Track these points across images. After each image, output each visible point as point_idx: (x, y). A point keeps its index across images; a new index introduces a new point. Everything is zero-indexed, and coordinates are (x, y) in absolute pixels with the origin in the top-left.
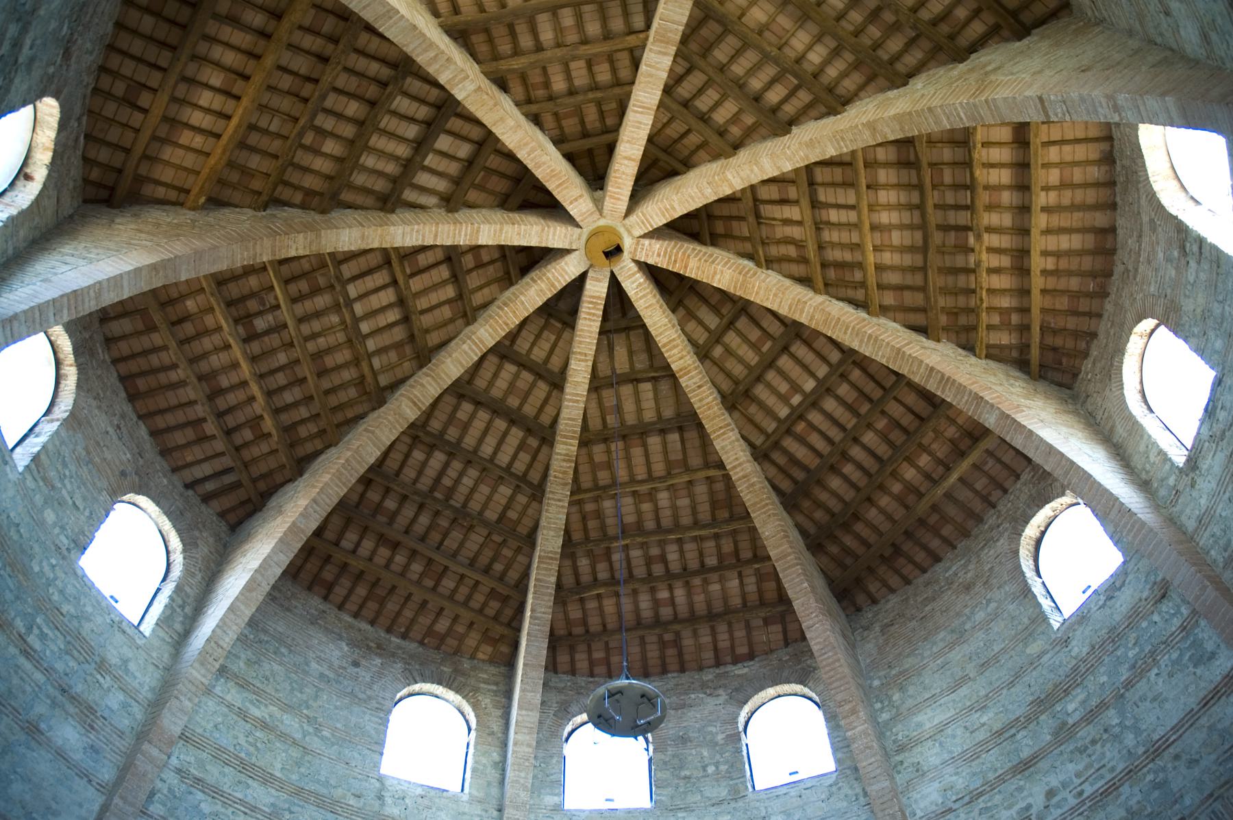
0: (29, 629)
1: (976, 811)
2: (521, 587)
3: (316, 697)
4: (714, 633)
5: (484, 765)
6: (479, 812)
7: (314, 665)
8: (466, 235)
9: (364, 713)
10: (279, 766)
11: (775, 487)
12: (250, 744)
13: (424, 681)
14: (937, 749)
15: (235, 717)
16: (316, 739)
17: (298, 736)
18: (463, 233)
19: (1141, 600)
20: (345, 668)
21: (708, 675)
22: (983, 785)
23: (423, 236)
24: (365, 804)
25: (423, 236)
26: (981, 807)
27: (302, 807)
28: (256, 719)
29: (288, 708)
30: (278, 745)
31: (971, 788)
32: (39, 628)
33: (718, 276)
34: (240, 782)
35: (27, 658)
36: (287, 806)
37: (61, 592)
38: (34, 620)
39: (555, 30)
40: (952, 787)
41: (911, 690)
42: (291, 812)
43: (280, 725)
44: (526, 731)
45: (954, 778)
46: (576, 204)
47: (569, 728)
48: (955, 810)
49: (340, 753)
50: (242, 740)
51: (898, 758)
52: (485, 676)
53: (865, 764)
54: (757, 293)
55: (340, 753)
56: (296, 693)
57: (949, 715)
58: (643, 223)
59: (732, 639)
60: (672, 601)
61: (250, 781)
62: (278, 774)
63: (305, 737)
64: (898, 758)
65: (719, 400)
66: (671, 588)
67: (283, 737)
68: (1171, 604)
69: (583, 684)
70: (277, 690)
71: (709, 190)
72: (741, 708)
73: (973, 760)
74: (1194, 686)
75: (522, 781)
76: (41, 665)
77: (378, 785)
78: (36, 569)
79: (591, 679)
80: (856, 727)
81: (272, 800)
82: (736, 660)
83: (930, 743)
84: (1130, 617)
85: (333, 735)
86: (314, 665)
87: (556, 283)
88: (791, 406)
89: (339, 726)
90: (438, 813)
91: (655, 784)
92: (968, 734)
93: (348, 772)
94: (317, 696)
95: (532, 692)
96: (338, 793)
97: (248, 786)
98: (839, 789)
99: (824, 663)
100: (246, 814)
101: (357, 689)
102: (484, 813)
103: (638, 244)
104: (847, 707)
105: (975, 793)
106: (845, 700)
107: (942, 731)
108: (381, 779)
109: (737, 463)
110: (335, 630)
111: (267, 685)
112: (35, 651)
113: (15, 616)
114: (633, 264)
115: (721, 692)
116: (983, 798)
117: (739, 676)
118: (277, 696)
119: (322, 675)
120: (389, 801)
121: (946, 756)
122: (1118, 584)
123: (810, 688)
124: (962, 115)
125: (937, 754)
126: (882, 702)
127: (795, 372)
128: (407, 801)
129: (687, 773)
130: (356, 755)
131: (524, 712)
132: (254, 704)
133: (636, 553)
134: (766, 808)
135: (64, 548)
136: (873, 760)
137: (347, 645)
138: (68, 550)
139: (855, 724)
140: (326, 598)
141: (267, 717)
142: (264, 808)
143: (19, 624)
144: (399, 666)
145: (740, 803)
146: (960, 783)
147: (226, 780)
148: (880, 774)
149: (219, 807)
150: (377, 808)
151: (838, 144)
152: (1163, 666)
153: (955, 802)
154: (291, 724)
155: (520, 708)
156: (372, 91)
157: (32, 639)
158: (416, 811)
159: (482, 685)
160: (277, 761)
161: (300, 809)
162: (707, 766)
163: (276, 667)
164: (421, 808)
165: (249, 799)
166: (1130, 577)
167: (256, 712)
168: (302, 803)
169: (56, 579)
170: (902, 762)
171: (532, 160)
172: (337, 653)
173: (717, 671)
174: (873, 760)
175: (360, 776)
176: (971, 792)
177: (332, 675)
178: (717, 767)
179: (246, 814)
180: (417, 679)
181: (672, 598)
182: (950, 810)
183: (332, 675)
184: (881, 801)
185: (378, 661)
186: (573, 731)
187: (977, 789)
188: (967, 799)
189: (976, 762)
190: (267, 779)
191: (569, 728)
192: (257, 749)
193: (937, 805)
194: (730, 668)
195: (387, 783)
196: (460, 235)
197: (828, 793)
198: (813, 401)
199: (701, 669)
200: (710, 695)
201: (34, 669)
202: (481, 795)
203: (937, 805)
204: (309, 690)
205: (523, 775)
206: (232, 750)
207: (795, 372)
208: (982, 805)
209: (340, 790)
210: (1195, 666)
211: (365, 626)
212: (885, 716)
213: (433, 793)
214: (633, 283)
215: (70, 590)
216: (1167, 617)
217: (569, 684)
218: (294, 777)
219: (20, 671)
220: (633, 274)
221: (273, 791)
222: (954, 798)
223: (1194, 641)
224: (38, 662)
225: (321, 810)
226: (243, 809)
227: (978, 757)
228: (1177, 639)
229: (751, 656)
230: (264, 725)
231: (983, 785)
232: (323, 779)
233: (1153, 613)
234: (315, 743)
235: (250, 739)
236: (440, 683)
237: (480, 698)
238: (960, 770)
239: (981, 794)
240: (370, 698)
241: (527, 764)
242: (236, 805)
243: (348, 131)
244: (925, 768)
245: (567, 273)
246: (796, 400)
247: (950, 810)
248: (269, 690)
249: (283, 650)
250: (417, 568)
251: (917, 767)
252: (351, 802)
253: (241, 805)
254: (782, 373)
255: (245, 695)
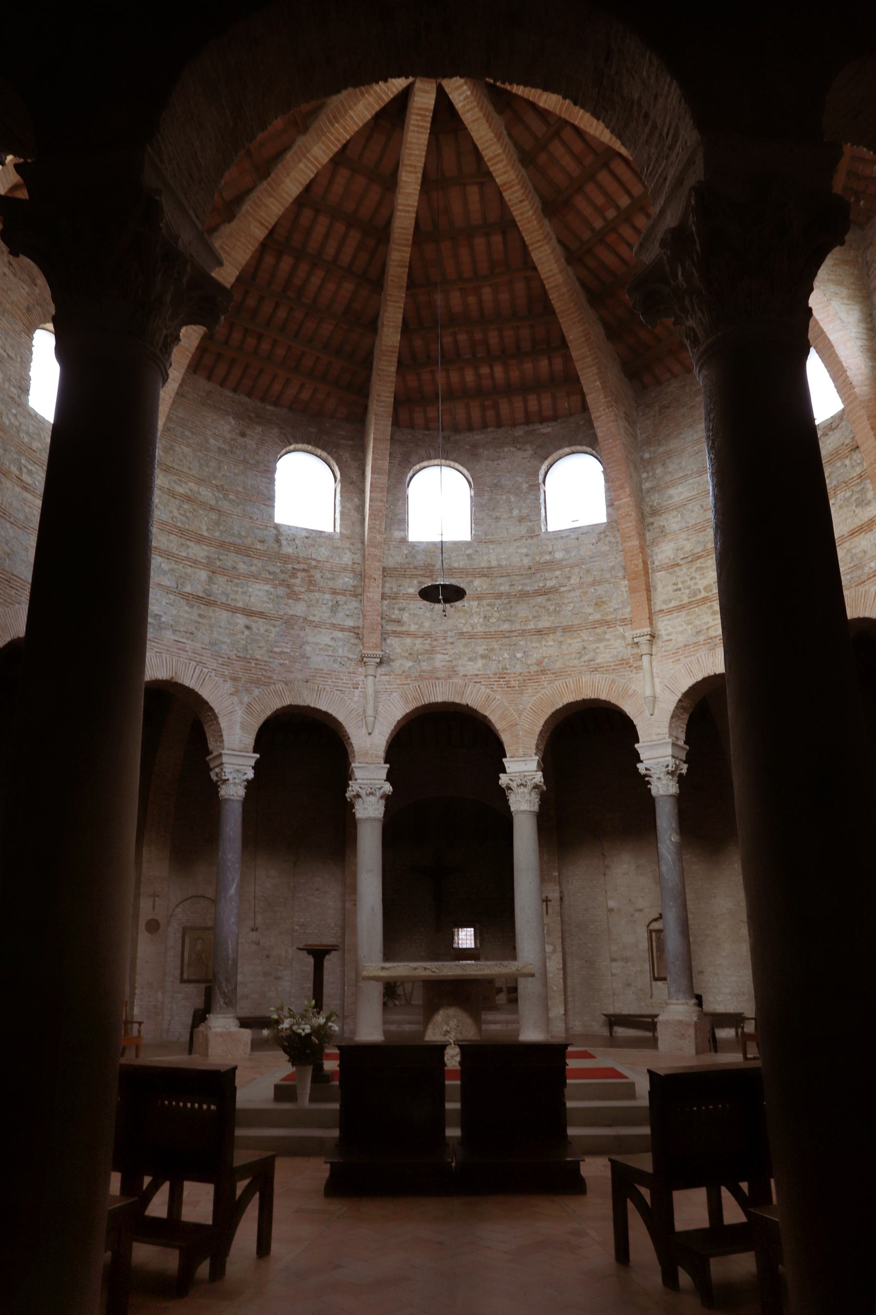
0: (20, 469)
1: (694, 568)
2: (367, 362)
3: (220, 468)
4: (525, 402)
5: (349, 509)
6: (348, 546)
7: (212, 441)
9: (256, 476)
10: (205, 528)
11: (583, 285)
12: (182, 515)
13: (297, 443)
14: (679, 518)
15: (167, 496)
16: (225, 502)
17: (213, 502)
19: (843, 444)
20: (235, 440)
21: (519, 432)
22: (702, 551)
24: (268, 547)
26: (697, 566)
27: (227, 555)
28: (181, 495)
29: (201, 481)
30: (201, 512)
31: (695, 551)
32: (26, 467)
34: (182, 545)
35: (27, 491)
36: (216, 556)
37: (27, 433)
38: (20, 462)
40: (682, 548)
41: (671, 467)
42: (220, 560)
43: (198, 496)
44: (378, 490)
45: (686, 542)
47: (410, 474)
48: (680, 565)
49: (244, 511)
50: (176, 513)
51: (651, 520)
52: (343, 433)
53: (624, 526)
55: (244, 511)
56: (204, 467)
57: (694, 493)
59: (540, 404)
60: (492, 375)
61: (188, 543)
62: (205, 534)
63: (217, 502)
64: (651, 520)
65: (540, 206)
66: (491, 367)
67: (203, 505)
68: (859, 456)
69: (421, 437)
70: (190, 468)
72: (542, 463)
73: (701, 532)
74: (850, 520)
75: (377, 527)
76: (37, 494)
77: (275, 532)
78: (7, 423)
79: (427, 432)
80: (622, 499)
81: (206, 554)
82: (543, 420)
83: (675, 513)
84: (832, 455)
85: (237, 497)
86: (212, 441)
88: (605, 219)
89: (240, 489)
90: (320, 549)
91: (476, 521)
92: (702, 511)
93: (252, 524)
94: (220, 468)
95: (381, 460)
96: (248, 541)
97: (188, 547)
98: (606, 536)
99: (605, 447)
100: (191, 566)
101: (247, 456)
102: (351, 547)
104: (617, 483)
105: (696, 555)
106: (616, 478)
107: (685, 505)
108: (277, 527)
109: (551, 274)
110: (222, 407)
111: (183, 465)
112: (29, 485)
113: (10, 465)
115: (528, 447)
116: (700, 560)
117: (544, 434)
118: (191, 473)
119: (220, 449)
120: (284, 542)
121: (683, 525)
122: (834, 425)
123: (596, 451)
125: (677, 522)
126: (648, 472)
127: (612, 186)
128: (297, 542)
129: (498, 514)
130: (256, 511)
131: (376, 476)
132: (177, 484)
133: (462, 337)
134: (553, 545)
135: (16, 397)
136: (630, 524)
137: (233, 418)
138: (19, 397)
139: (622, 497)
140: (209, 378)
141: (188, 491)
142: (202, 560)
143: (14, 469)
144: (276, 430)
145: (535, 540)
146: (688, 546)
147: (173, 545)
148: (633, 535)
149: (173, 566)
150: (276, 549)
152: (838, 500)
153: (682, 559)
154: (206, 494)
155: (373, 472)
157: (25, 477)
158: (304, 548)
159: (342, 442)
160: (203, 524)
161: (225, 557)
162: (513, 509)
163: (186, 449)
164: (307, 546)
165: (191, 555)
166: (843, 423)
167: (180, 490)
168: (225, 553)
169: (20, 424)
170: (652, 524)
172: (227, 427)
173: (527, 428)
174: (630, 524)
175: (261, 527)
176: (694, 554)
177: (227, 448)
178: (520, 511)
179: (191, 566)
180: (291, 441)
181: (492, 374)
182: (678, 565)
183: (227, 448)
184: (631, 554)
185: (259, 429)
186: (414, 475)
187: (698, 553)
188: (690, 559)
189: (703, 533)
190: (200, 539)
191: (410, 474)
192: (187, 517)
193: (669, 559)
194: (537, 426)
195: (281, 530)
197: (597, 539)
198: (626, 216)
199: (514, 425)
200: (519, 449)
201: (34, 498)
202: (347, 532)
203: (669, 559)
204: (213, 464)
205: (378, 522)
206: (171, 522)
207: (612, 186)
208: (699, 565)
209: (249, 539)
210: (857, 506)
211: (246, 399)
212: (647, 485)
213: (314, 534)
215: (31, 429)
216: (854, 464)
217: (409, 437)
218: (217, 534)
219: (27, 502)
221: (205, 547)
222: (682, 556)
223: (863, 488)
224: (34, 492)
225: (240, 556)
226: (189, 563)
227: (704, 530)
228: (854, 483)
229: (555, 418)
230: (188, 499)
231: (702, 551)
232: (236, 533)
233: (847, 457)
234: (225, 506)
235: (182, 512)
236: (309, 443)
237: (341, 453)
238: (691, 536)
239: (699, 557)
240: (258, 462)
241: (380, 514)
242: (184, 562)
244: (668, 531)
246: (611, 214)
247: (678, 565)
248: (185, 469)
249: (187, 433)
250: (280, 352)
251: (662, 529)
252: (258, 547)
253: (186, 560)
254: (600, 187)
255: (169, 477)
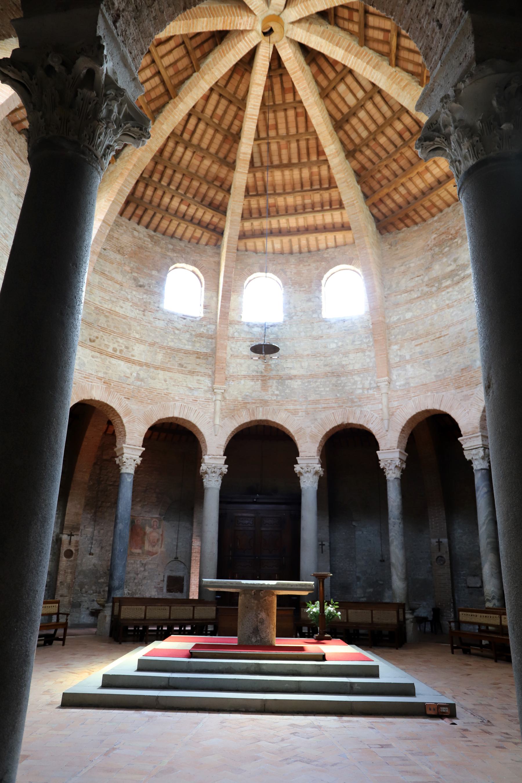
8: (350, 60)
18: (351, 62)
23: (371, 73)
25: (371, 73)
33: (204, 25)
39: (290, 148)
46: (288, 57)
54: (180, 27)
58: (250, 41)
71: (216, 74)
87: (304, 8)
103: (253, 27)
114: (256, 13)
124: (125, 189)
151: (162, 133)
156: (372, 143)
171: (307, 94)
196: (352, 62)
214: (255, 5)
220: (255, 9)
243: (389, 131)
245: (297, 12)
